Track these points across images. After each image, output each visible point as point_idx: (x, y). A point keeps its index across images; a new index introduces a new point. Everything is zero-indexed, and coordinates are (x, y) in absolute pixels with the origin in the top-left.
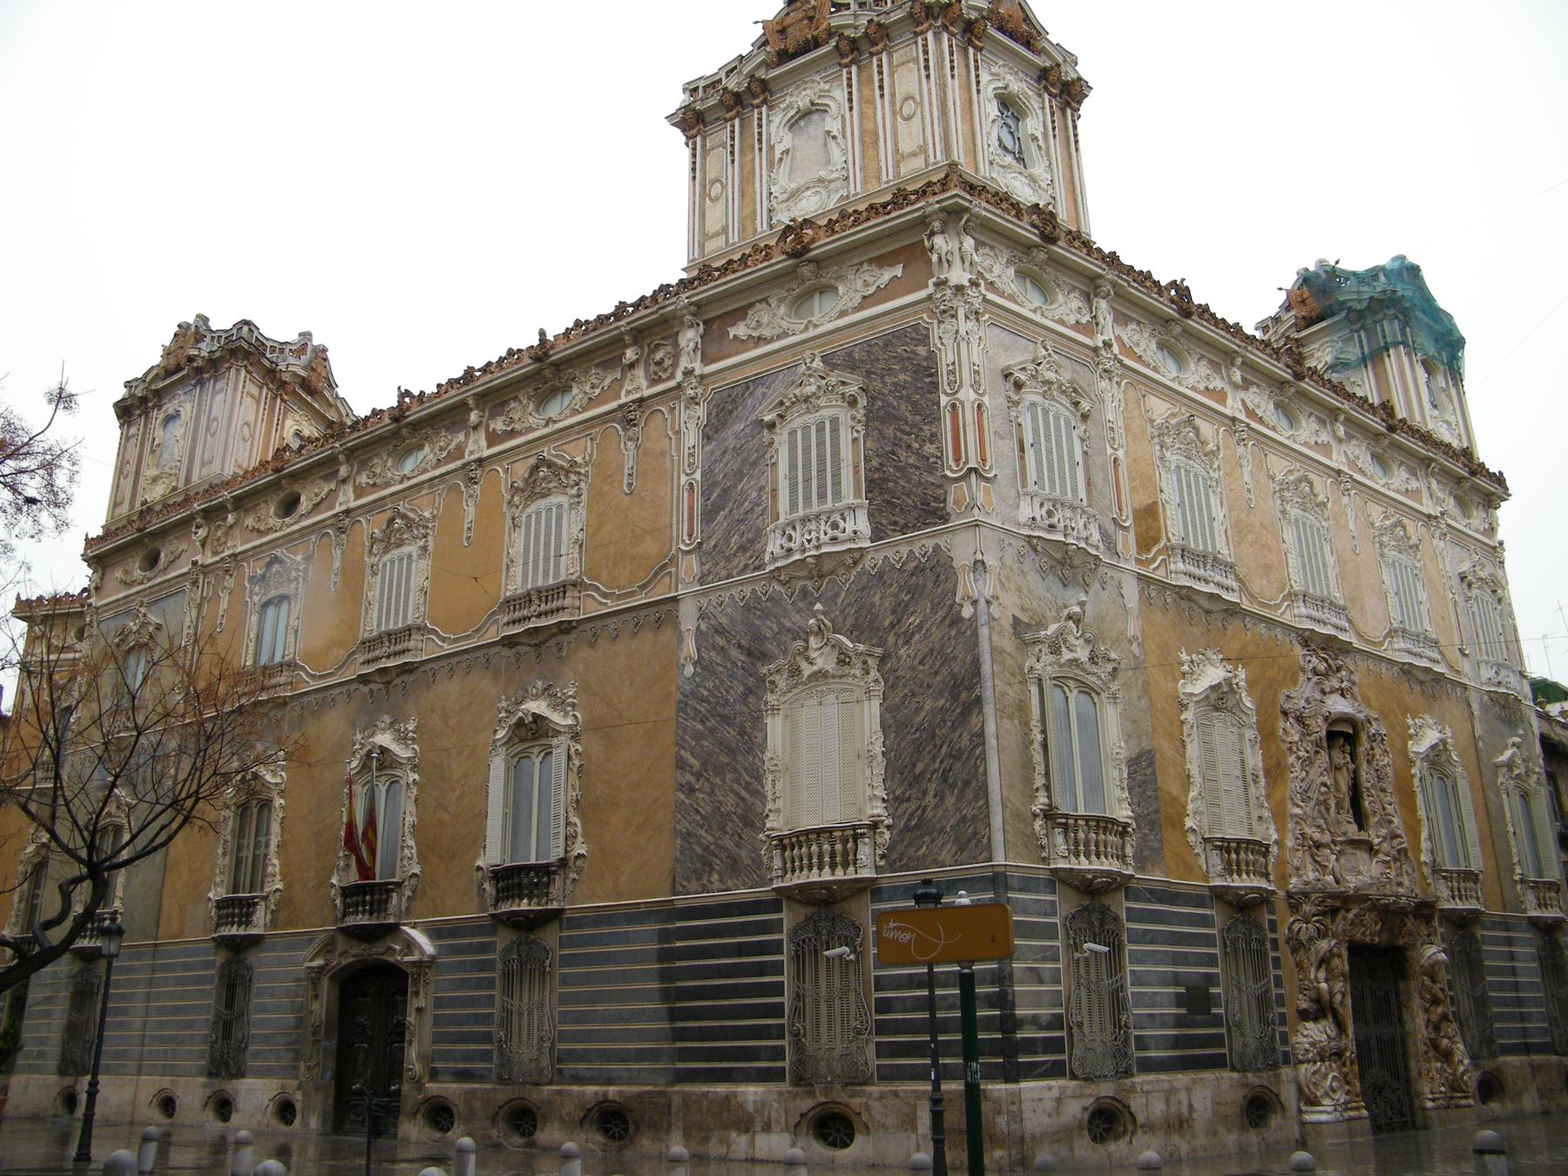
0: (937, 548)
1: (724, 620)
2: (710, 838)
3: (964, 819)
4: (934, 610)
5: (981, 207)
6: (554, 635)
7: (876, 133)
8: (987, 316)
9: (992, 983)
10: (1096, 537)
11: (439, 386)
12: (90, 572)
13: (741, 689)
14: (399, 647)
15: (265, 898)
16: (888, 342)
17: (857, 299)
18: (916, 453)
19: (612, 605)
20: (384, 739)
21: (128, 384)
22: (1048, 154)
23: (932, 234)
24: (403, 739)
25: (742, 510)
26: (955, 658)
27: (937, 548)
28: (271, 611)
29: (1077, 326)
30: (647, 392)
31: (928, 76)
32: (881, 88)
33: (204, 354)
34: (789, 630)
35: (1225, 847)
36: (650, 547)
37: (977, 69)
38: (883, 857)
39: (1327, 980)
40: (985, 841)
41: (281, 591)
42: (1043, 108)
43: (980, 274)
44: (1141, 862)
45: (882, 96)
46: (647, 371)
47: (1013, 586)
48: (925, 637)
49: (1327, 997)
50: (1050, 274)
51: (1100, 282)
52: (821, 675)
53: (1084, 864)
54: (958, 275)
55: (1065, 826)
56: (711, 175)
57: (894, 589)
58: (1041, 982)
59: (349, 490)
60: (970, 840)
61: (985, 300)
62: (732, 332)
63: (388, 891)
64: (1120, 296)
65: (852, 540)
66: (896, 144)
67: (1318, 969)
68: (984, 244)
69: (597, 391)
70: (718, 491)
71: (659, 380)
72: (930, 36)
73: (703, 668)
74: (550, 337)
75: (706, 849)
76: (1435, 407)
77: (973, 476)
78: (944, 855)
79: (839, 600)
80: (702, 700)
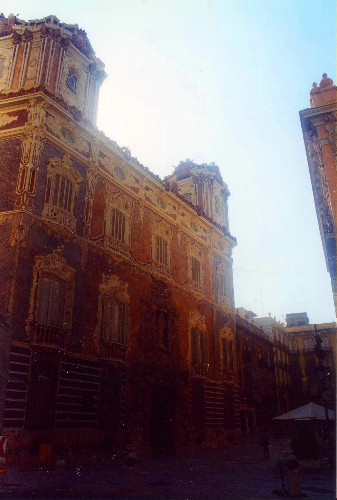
5: (48, 99)
8: (45, 140)
10: (74, 226)
23: (30, 107)
31: (42, 53)
32: (26, 54)
37: (63, 55)
42: (87, 77)
43: (45, 125)
61: (45, 133)
68: (50, 115)
72: (46, 39)
76: (217, 212)
77: (25, 194)
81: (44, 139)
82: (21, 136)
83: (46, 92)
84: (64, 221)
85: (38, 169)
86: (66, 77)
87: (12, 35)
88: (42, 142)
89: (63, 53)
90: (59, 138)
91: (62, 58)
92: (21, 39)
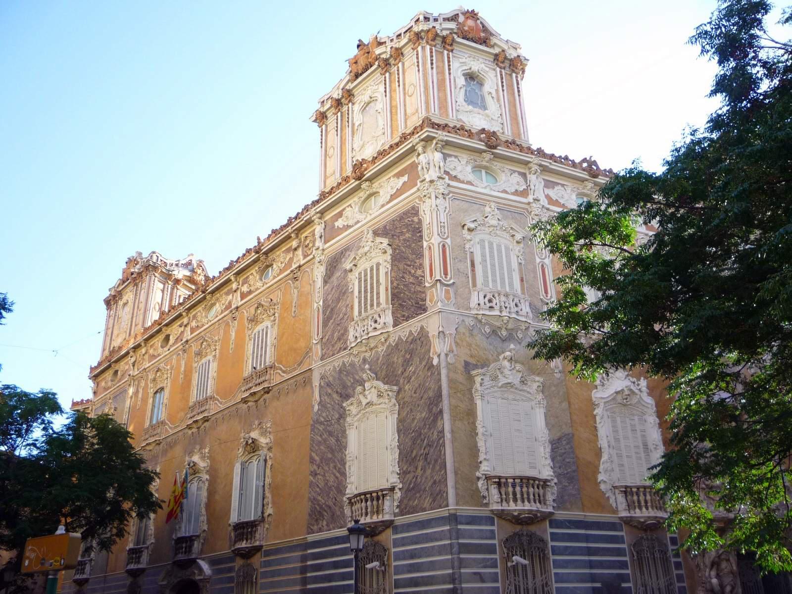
0: (422, 328)
1: (331, 379)
2: (323, 501)
3: (435, 482)
4: (421, 363)
5: (441, 135)
6: (263, 395)
7: (397, 107)
8: (451, 195)
9: (450, 583)
11: (220, 272)
12: (92, 385)
13: (337, 416)
14: (203, 408)
15: (147, 548)
16: (401, 218)
17: (389, 197)
18: (413, 276)
19: (287, 377)
20: (196, 458)
21: (110, 290)
22: (498, 100)
23: (419, 155)
24: (203, 458)
25: (339, 319)
26: (430, 388)
27: (422, 328)
28: (158, 395)
29: (516, 193)
30: (302, 262)
33: (137, 270)
34: (357, 381)
35: (627, 491)
36: (302, 344)
37: (449, 61)
38: (398, 507)
39: (718, 576)
40: (445, 495)
41: (161, 386)
42: (496, 76)
43: (446, 173)
44: (561, 502)
45: (399, 86)
46: (303, 251)
47: (465, 344)
48: (416, 379)
49: (717, 588)
50: (497, 165)
51: (530, 165)
52: (370, 404)
53: (512, 506)
54: (433, 174)
55: (499, 484)
56: (329, 145)
57: (403, 353)
58: (483, 580)
59: (188, 329)
60: (437, 495)
61: (449, 185)
62: (336, 224)
63: (193, 540)
64: (545, 169)
65: (383, 328)
66: (405, 111)
67: (711, 569)
68: (450, 156)
69: (283, 265)
70: (329, 309)
71: (308, 255)
72: (419, 49)
73: (322, 406)
74: (262, 241)
75: (321, 507)
77: (438, 284)
78: (426, 504)
79: (379, 361)
80: (321, 423)
81: (448, 194)
82: (417, 201)
83: (434, 125)
84: (506, 308)
85: (448, 241)
86: (463, 91)
87: (377, 63)
88: (447, 199)
89: (449, 58)
90: (473, 185)
91: (449, 66)
92: (390, 64)
